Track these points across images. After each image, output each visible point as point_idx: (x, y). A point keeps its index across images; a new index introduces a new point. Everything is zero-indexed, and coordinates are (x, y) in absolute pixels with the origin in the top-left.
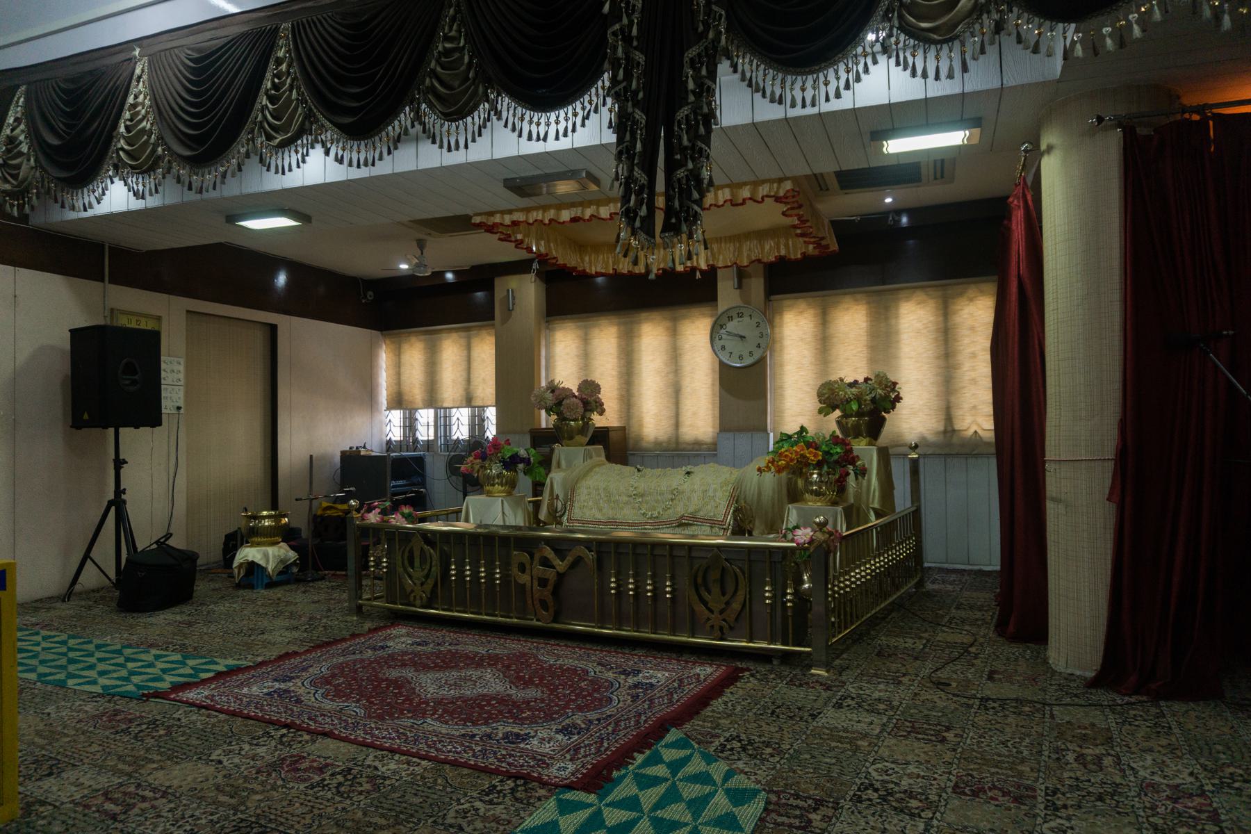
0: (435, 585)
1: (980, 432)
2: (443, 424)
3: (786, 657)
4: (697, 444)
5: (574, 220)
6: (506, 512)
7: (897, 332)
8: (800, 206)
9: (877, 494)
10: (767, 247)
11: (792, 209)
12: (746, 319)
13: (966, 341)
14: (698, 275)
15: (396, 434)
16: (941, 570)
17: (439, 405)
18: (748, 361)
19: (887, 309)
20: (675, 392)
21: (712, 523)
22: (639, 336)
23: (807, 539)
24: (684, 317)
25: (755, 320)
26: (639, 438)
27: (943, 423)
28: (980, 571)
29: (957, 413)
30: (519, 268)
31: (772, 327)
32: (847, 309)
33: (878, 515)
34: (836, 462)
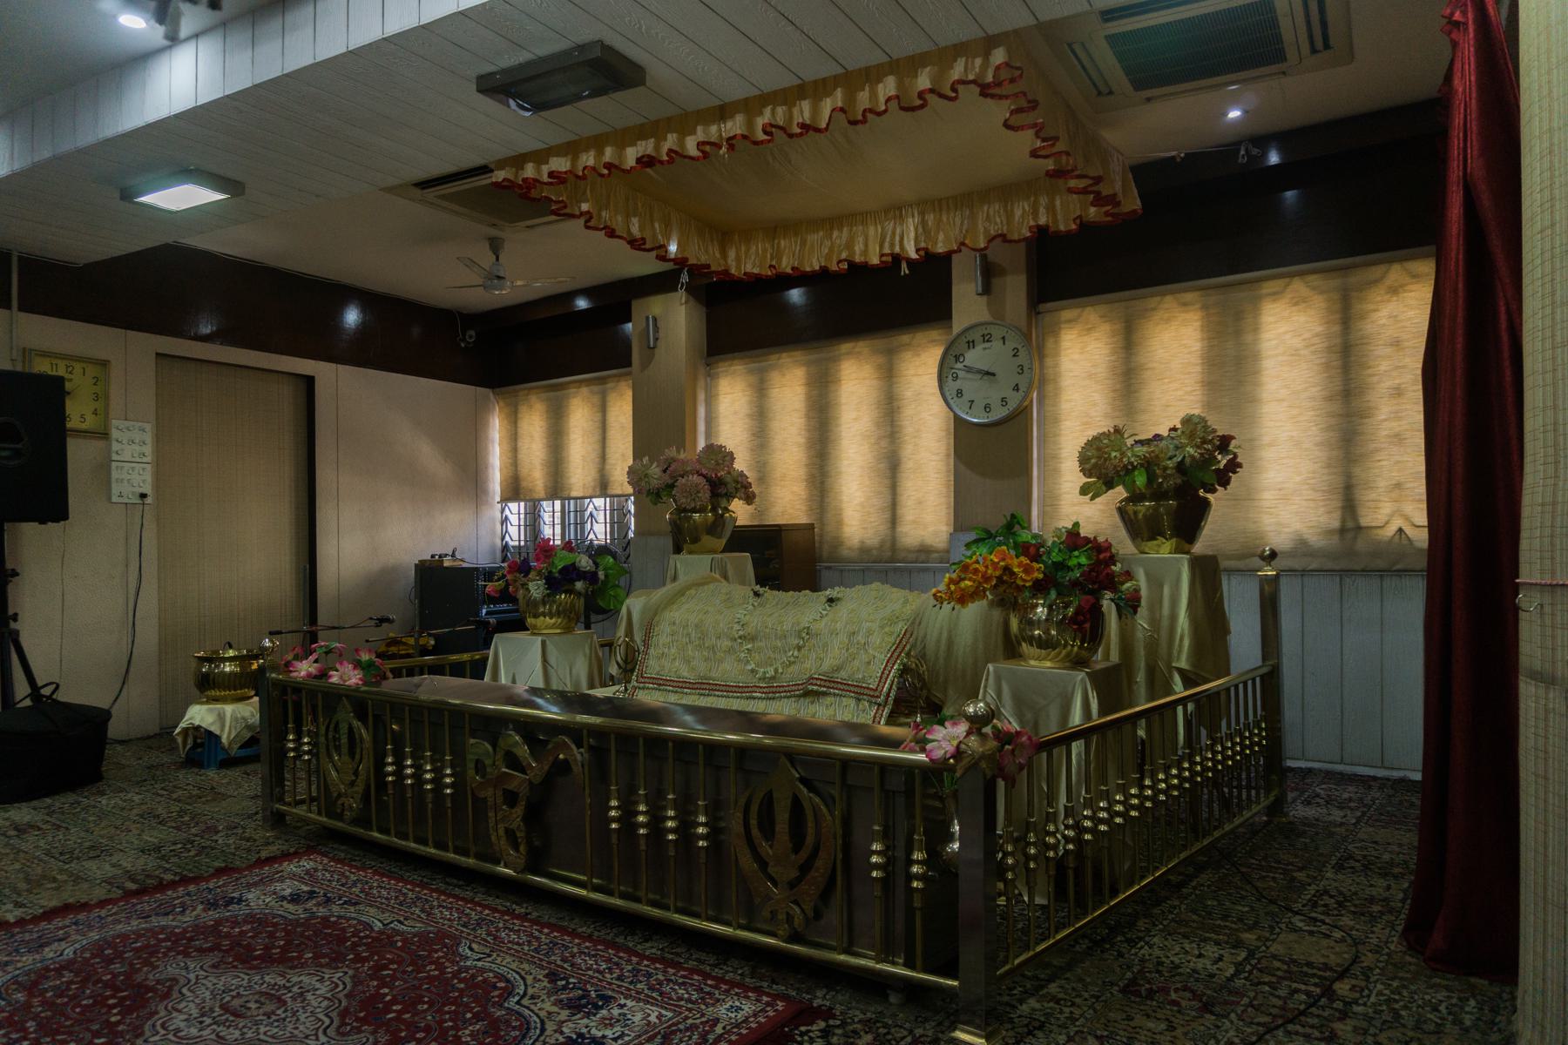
0: (368, 787)
1: (1409, 530)
2: (576, 519)
3: (914, 993)
4: (924, 551)
5: (646, 162)
6: (552, 660)
7: (1256, 357)
8: (1034, 105)
9: (1186, 643)
10: (1018, 213)
11: (1019, 110)
12: (996, 344)
13: (1384, 366)
14: (905, 269)
15: (515, 535)
16: (1329, 774)
17: (565, 494)
18: (999, 413)
19: (1239, 316)
20: (891, 468)
21: (860, 692)
22: (838, 381)
23: (949, 748)
24: (908, 346)
25: (1011, 345)
26: (838, 542)
27: (1337, 515)
28: (1403, 780)
29: (1365, 497)
30: (661, 283)
31: (1042, 357)
32: (1168, 320)
33: (1189, 681)
34: (1075, 584)
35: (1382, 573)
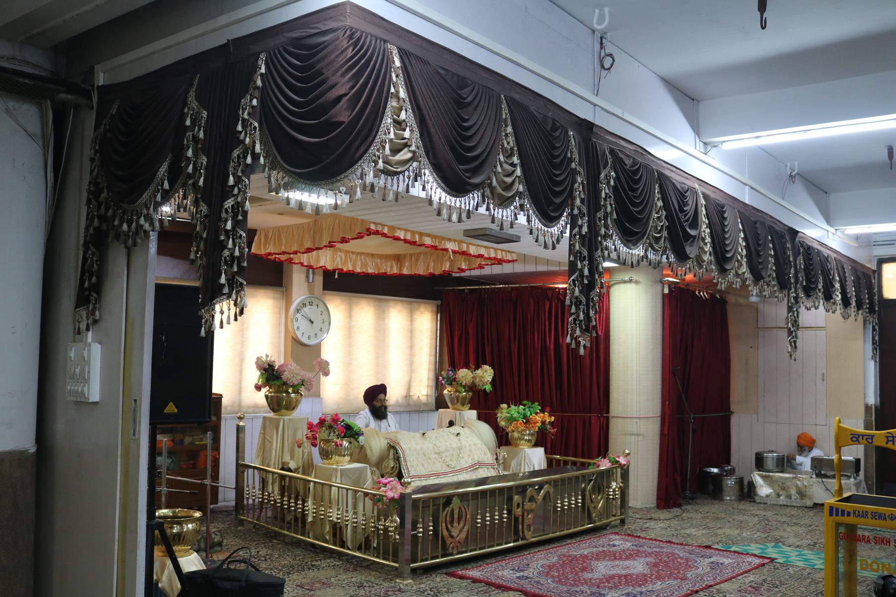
12: (314, 307)
19: (384, 311)
29: (413, 384)
35: (419, 412)
